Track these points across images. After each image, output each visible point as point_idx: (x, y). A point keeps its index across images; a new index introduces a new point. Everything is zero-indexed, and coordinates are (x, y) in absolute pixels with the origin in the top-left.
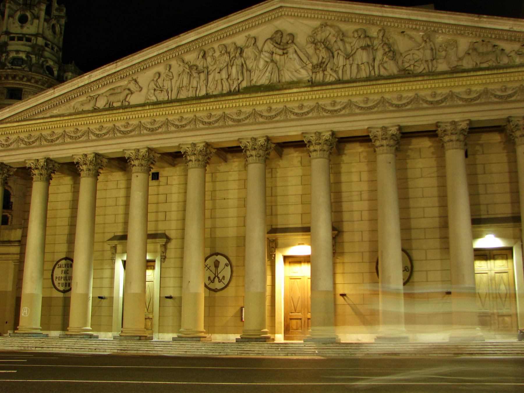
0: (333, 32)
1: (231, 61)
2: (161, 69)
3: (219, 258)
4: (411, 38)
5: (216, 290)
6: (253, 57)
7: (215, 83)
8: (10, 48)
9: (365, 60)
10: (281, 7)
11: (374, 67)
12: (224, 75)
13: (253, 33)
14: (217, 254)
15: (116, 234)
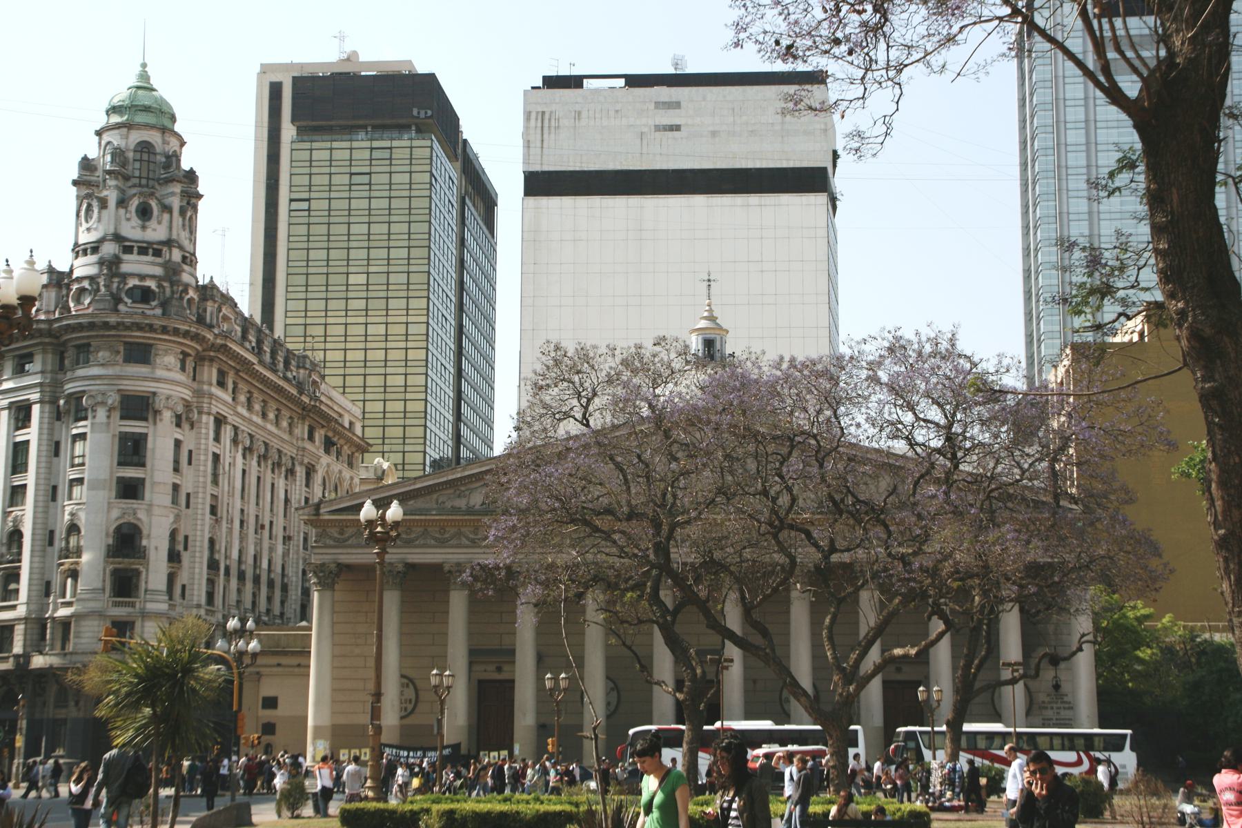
8: (125, 268)
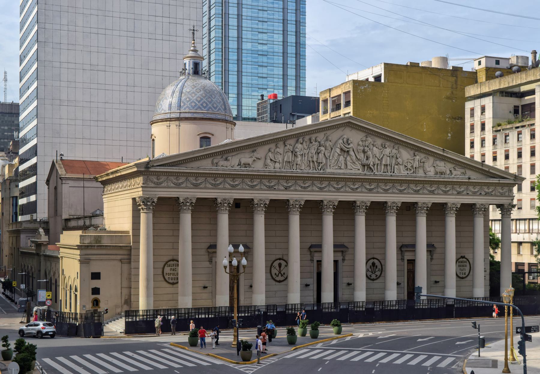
0: (372, 143)
1: (318, 149)
2: (273, 146)
3: (282, 262)
4: (409, 153)
5: (280, 281)
6: (330, 149)
9: (388, 163)
10: (349, 122)
12: (315, 159)
13: (329, 132)
14: (280, 259)
15: (211, 244)
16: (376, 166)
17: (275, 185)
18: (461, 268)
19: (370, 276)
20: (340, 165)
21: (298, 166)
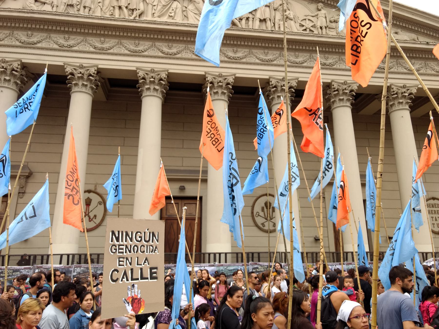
3: (92, 196)
7: (112, 8)
9: (267, 16)
11: (274, 24)
14: (89, 191)
16: (244, 21)
17: (39, 42)
18: (434, 216)
19: (263, 224)
20: (172, 14)
21: (87, 10)
